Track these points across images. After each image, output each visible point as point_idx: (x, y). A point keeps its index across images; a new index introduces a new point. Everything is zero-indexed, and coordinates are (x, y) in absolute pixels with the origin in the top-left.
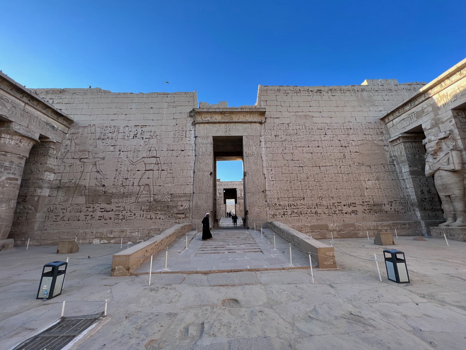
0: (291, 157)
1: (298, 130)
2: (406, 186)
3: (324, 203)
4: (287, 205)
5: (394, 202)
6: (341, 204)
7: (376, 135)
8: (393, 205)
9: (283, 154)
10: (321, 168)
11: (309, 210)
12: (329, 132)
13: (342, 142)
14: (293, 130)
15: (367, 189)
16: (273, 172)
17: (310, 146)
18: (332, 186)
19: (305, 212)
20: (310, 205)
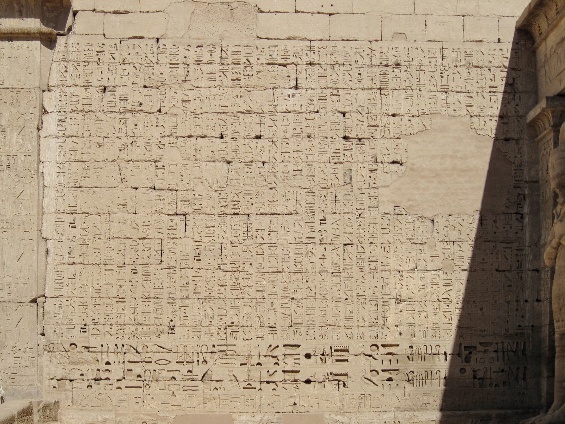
0: (152, 176)
1: (192, 67)
2: (538, 291)
3: (241, 347)
4: (112, 348)
5: (480, 348)
6: (297, 351)
7: (487, 95)
8: (473, 357)
9: (123, 165)
10: (253, 218)
11: (184, 369)
12: (310, 78)
13: (352, 119)
14: (174, 65)
15: (399, 301)
16: (77, 232)
17: (229, 134)
18: (279, 290)
19: (170, 374)
20: (190, 349)
